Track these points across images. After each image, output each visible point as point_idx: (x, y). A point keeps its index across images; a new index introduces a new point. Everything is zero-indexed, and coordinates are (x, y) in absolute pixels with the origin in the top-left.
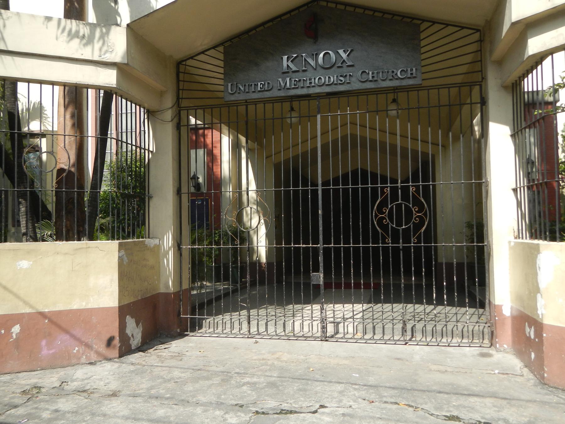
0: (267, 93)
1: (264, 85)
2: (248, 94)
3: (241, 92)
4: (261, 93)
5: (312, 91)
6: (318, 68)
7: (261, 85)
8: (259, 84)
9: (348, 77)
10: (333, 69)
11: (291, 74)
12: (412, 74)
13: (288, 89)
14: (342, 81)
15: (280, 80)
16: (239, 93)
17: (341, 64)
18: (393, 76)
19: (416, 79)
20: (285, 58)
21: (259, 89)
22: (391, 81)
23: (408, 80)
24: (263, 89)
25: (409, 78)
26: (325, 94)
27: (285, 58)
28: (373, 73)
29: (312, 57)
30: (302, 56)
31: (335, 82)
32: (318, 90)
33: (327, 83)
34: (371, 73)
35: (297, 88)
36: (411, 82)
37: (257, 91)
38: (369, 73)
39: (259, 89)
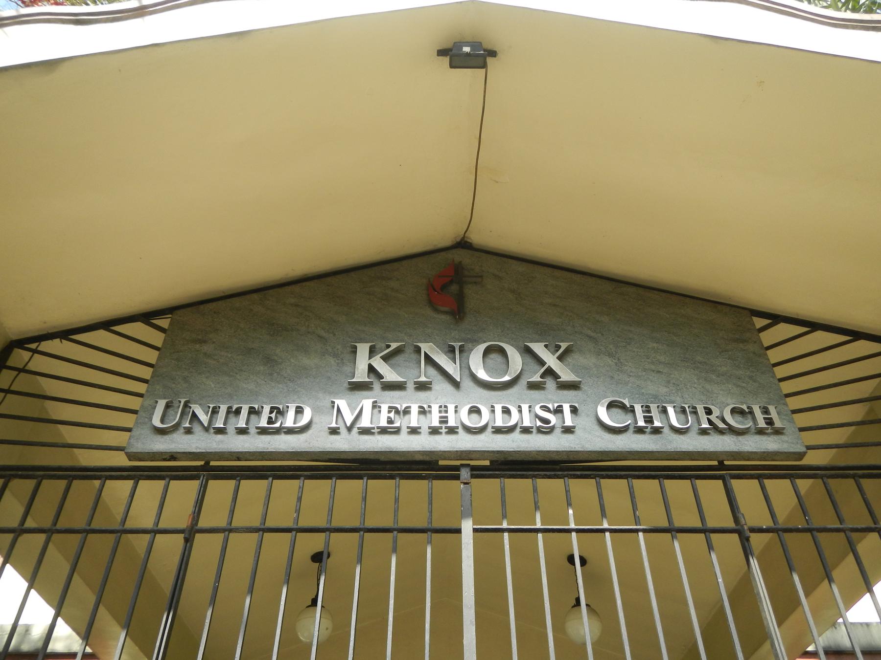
0: (289, 438)
1: (281, 413)
3: (197, 428)
5: (443, 443)
6: (467, 383)
8: (267, 409)
12: (770, 422)
14: (547, 421)
15: (342, 403)
16: (189, 431)
17: (541, 377)
18: (710, 422)
20: (363, 349)
21: (263, 423)
22: (706, 437)
23: (758, 438)
24: (277, 425)
25: (761, 432)
26: (487, 463)
27: (363, 349)
28: (647, 409)
29: (451, 355)
31: (527, 423)
32: (464, 442)
33: (499, 423)
34: (638, 408)
35: (397, 431)
36: (769, 444)
37: (253, 430)
38: (632, 407)
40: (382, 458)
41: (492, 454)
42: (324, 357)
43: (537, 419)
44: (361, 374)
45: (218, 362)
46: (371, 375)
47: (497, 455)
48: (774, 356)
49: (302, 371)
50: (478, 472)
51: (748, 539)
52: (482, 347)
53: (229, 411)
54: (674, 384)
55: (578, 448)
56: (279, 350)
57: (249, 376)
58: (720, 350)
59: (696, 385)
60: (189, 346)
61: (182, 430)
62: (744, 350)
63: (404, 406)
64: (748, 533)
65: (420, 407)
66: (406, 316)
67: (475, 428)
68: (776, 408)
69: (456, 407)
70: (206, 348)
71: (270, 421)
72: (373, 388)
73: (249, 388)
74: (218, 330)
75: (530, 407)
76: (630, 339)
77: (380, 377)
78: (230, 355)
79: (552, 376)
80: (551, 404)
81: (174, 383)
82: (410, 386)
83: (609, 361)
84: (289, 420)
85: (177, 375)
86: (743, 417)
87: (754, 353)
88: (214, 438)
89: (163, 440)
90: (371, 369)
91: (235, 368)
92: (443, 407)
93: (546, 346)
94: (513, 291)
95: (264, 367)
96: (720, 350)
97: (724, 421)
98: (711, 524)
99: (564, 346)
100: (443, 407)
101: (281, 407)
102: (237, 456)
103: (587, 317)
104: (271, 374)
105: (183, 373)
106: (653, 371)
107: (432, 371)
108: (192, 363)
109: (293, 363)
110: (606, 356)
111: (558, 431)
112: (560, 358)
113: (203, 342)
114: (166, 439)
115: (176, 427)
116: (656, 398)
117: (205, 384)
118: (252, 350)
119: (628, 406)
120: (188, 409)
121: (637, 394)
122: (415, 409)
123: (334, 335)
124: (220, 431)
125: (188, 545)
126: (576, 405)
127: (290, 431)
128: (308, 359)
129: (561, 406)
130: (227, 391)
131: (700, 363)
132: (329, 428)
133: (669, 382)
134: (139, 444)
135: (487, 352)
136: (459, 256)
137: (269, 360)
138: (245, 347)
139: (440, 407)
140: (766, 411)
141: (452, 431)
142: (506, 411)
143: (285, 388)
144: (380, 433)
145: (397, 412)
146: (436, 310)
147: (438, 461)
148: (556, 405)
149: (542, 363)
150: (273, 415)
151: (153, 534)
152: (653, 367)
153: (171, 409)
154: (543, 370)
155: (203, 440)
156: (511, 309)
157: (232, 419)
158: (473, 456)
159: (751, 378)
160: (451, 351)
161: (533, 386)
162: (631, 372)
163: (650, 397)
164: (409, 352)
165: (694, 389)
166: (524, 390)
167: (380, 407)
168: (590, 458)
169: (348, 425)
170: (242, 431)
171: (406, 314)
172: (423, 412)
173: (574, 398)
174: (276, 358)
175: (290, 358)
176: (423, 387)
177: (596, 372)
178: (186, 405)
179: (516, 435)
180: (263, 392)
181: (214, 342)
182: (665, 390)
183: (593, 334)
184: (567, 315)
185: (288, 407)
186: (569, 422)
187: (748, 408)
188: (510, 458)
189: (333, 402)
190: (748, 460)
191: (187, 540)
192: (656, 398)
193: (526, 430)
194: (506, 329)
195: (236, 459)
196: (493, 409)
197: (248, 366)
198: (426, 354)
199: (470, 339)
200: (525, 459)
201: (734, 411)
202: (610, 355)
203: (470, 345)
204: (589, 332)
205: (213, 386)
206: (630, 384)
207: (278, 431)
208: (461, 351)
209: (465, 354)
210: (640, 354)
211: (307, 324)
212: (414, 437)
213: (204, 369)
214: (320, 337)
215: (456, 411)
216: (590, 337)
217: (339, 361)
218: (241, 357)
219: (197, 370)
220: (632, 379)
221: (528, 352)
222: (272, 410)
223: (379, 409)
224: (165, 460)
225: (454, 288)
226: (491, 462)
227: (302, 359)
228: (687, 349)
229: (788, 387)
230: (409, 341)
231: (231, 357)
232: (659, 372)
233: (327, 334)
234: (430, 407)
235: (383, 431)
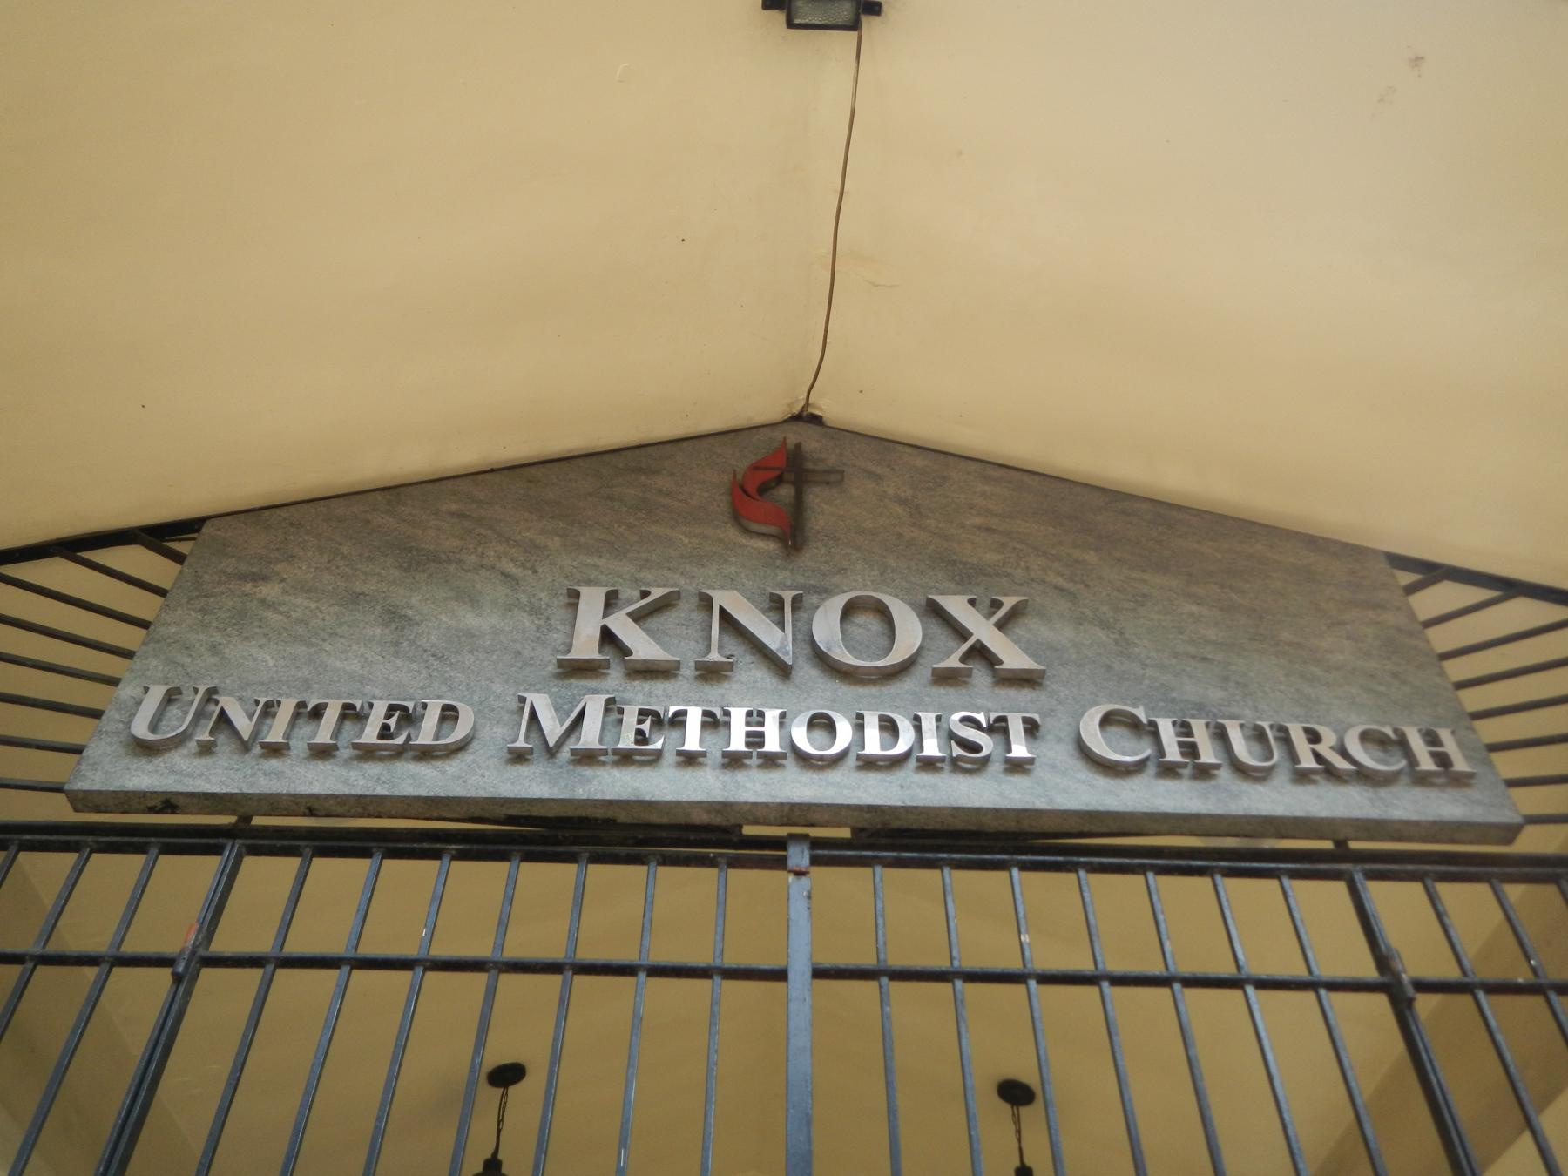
1: (409, 718)
2: (274, 763)
4: (373, 769)
5: (753, 788)
6: (807, 672)
7: (388, 716)
8: (380, 708)
9: (1016, 727)
10: (907, 685)
11: (615, 678)
12: (1443, 760)
13: (587, 758)
14: (975, 748)
15: (541, 703)
16: (206, 749)
17: (963, 659)
18: (1318, 757)
19: (1474, 793)
20: (592, 600)
21: (370, 735)
23: (1418, 792)
26: (845, 833)
27: (592, 600)
28: (1184, 729)
30: (706, 603)
31: (932, 748)
38: (1153, 724)
39: (370, 735)
40: (622, 817)
41: (856, 814)
42: (510, 614)
43: (953, 742)
44: (586, 646)
45: (288, 617)
46: (607, 649)
47: (867, 816)
48: (1443, 638)
49: (463, 639)
50: (827, 854)
51: (1410, 1002)
52: (837, 603)
53: (297, 715)
54: (1237, 683)
55: (1040, 804)
56: (418, 598)
57: (350, 647)
58: (1329, 621)
59: (1283, 687)
60: (231, 586)
61: (192, 746)
62: (1378, 623)
63: (673, 709)
64: (1410, 991)
65: (706, 713)
66: (686, 541)
67: (821, 758)
68: (1453, 733)
69: (783, 716)
70: (270, 591)
71: (385, 732)
72: (608, 674)
73: (348, 668)
74: (295, 556)
75: (938, 719)
76: (1144, 596)
77: (624, 651)
78: (313, 606)
79: (983, 662)
80: (982, 714)
81: (190, 656)
82: (688, 671)
83: (1102, 635)
84: (426, 734)
85: (199, 640)
86: (1385, 751)
87: (1399, 630)
88: (261, 767)
89: (149, 767)
90: (607, 637)
91: (324, 630)
92: (755, 714)
93: (972, 602)
94: (903, 502)
95: (382, 630)
96: (1329, 621)
97: (1344, 753)
98: (1324, 971)
99: (1009, 602)
100: (755, 714)
101: (410, 705)
102: (309, 805)
103: (1054, 552)
104: (397, 644)
105: (212, 636)
106: (1193, 657)
107: (736, 648)
108: (233, 618)
109: (445, 622)
110: (1095, 625)
111: (996, 767)
112: (1001, 625)
113: (259, 578)
114: (158, 766)
115: (180, 741)
116: (1200, 709)
117: (255, 660)
118: (361, 597)
119: (1144, 721)
120: (211, 707)
121: (1161, 700)
122: (694, 717)
123: (535, 572)
124: (275, 750)
125: (181, 989)
126: (1037, 717)
127: (426, 754)
128: (477, 615)
129: (1003, 719)
130: (300, 674)
131: (1290, 644)
132: (511, 750)
133: (1226, 679)
134: (98, 773)
135: (849, 611)
136: (794, 435)
137: (394, 617)
138: (346, 591)
139: (749, 714)
140: (1432, 739)
141: (771, 761)
142: (889, 727)
143: (424, 671)
144: (617, 764)
145: (658, 721)
146: (747, 531)
147: (740, 827)
148: (993, 716)
149: (962, 633)
150: (392, 722)
151: (105, 967)
152: (1192, 650)
153: (178, 705)
154: (965, 647)
155: (238, 770)
156: (901, 534)
157: (305, 729)
158: (816, 817)
159: (1395, 675)
160: (776, 605)
161: (946, 678)
162: (1148, 658)
163: (1190, 706)
164: (686, 610)
165: (1278, 693)
166: (925, 687)
167: (621, 711)
168: (1066, 828)
169: (551, 743)
170: (322, 753)
171: (686, 536)
172: (714, 723)
173: (1030, 705)
174: (409, 613)
175: (441, 613)
176: (711, 673)
177: (1074, 656)
178: (211, 695)
179: (908, 773)
180: (378, 677)
181: (283, 580)
182: (1221, 694)
183: (1065, 585)
184: (1014, 548)
185: (425, 706)
186: (1020, 750)
187: (1396, 731)
188: (896, 824)
189: (522, 700)
190: (1400, 839)
191: (178, 979)
192: (1200, 709)
193: (929, 764)
194: (889, 571)
195: (307, 812)
196: (860, 721)
197: (349, 626)
198: (722, 611)
199: (815, 587)
200: (926, 828)
201: (1365, 737)
202: (1104, 625)
203: (814, 599)
204: (1060, 581)
205: (271, 663)
206: (1147, 682)
207: (399, 753)
208: (794, 609)
209: (804, 615)
210: (1164, 624)
211: (480, 550)
212: (688, 775)
213: (257, 630)
214: (506, 576)
215: (781, 724)
216: (1062, 590)
217: (542, 622)
218: (337, 608)
219: (241, 632)
220: (1149, 672)
221: (934, 612)
222: (392, 709)
223: (620, 716)
224: (151, 810)
225: (785, 492)
226: (856, 831)
227: (464, 617)
228: (1261, 618)
229: (1474, 699)
230: (690, 588)
231: (317, 608)
232: (1205, 659)
233: (520, 570)
234: (727, 714)
235: (625, 758)
